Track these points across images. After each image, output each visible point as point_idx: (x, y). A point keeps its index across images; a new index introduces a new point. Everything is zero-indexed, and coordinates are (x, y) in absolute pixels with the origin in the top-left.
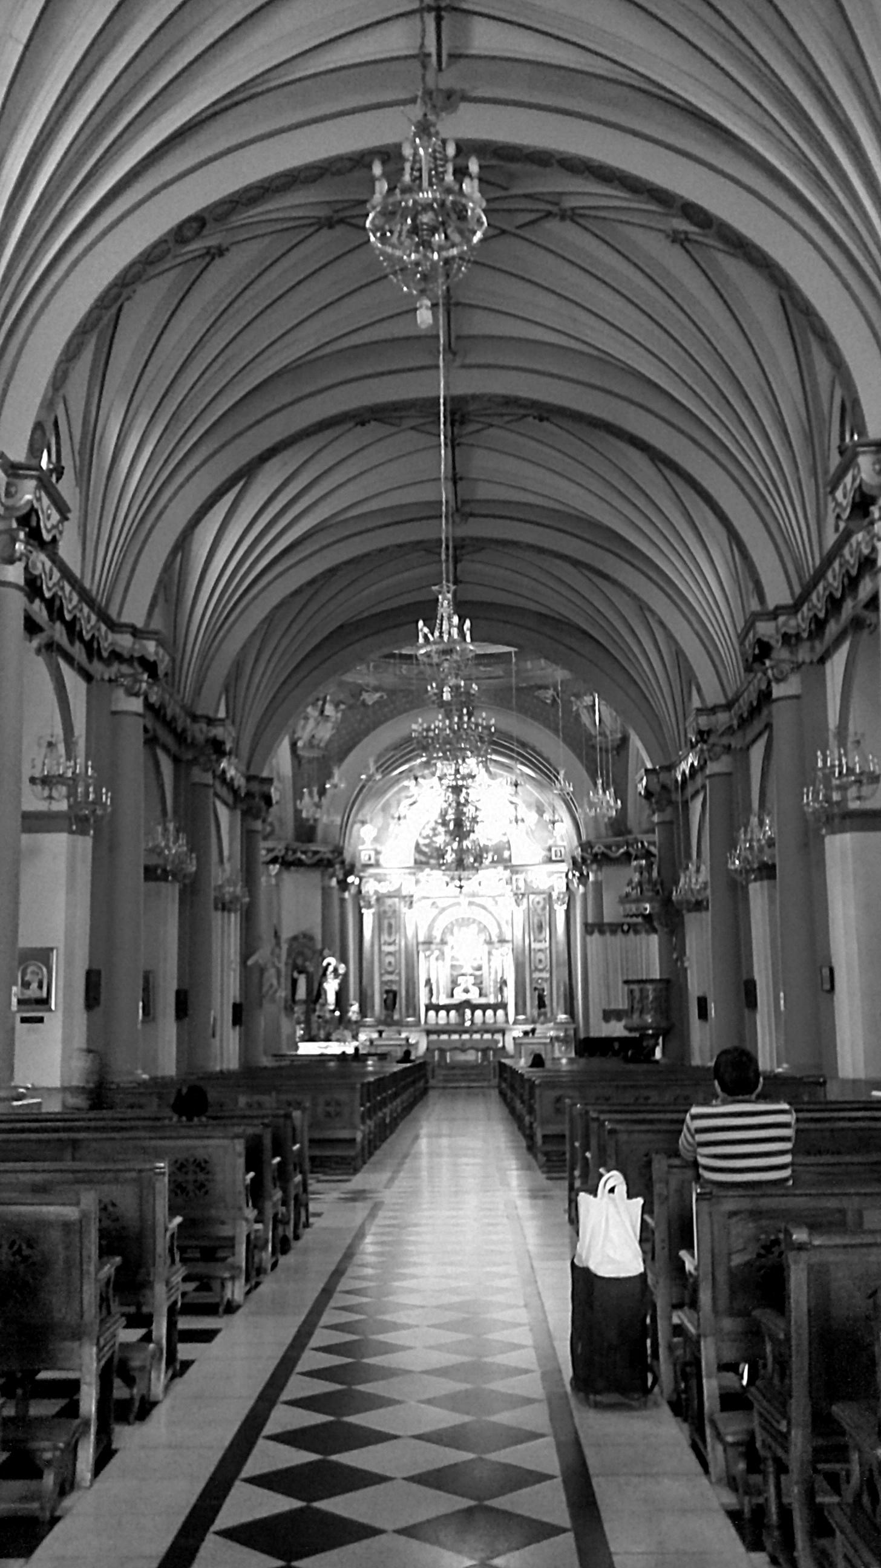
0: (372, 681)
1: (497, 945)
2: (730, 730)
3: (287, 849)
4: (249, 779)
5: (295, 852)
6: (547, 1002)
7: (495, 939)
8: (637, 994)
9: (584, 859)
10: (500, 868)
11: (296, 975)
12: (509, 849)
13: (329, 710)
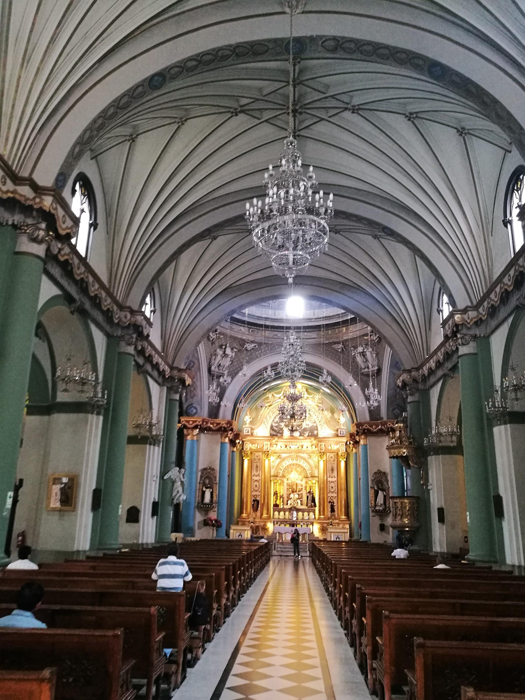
0: (251, 338)
1: (310, 479)
2: (478, 323)
3: (203, 421)
4: (172, 368)
5: (207, 423)
6: (336, 509)
7: (309, 475)
8: (399, 505)
9: (358, 433)
10: (313, 439)
11: (204, 489)
12: (317, 430)
13: (228, 351)
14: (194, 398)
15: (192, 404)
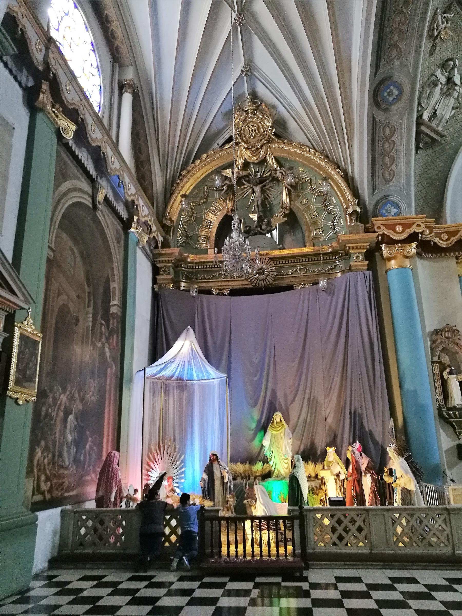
14: (392, 183)
15: (387, 196)
